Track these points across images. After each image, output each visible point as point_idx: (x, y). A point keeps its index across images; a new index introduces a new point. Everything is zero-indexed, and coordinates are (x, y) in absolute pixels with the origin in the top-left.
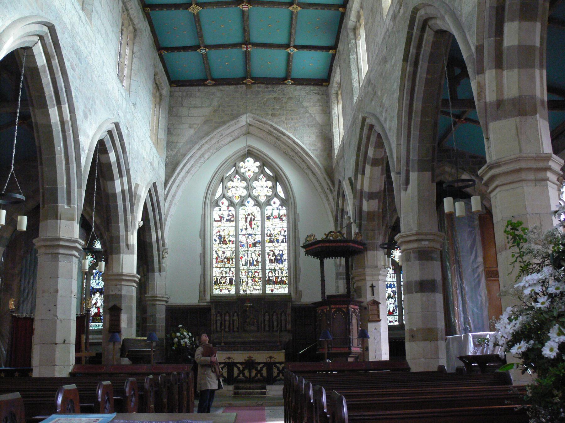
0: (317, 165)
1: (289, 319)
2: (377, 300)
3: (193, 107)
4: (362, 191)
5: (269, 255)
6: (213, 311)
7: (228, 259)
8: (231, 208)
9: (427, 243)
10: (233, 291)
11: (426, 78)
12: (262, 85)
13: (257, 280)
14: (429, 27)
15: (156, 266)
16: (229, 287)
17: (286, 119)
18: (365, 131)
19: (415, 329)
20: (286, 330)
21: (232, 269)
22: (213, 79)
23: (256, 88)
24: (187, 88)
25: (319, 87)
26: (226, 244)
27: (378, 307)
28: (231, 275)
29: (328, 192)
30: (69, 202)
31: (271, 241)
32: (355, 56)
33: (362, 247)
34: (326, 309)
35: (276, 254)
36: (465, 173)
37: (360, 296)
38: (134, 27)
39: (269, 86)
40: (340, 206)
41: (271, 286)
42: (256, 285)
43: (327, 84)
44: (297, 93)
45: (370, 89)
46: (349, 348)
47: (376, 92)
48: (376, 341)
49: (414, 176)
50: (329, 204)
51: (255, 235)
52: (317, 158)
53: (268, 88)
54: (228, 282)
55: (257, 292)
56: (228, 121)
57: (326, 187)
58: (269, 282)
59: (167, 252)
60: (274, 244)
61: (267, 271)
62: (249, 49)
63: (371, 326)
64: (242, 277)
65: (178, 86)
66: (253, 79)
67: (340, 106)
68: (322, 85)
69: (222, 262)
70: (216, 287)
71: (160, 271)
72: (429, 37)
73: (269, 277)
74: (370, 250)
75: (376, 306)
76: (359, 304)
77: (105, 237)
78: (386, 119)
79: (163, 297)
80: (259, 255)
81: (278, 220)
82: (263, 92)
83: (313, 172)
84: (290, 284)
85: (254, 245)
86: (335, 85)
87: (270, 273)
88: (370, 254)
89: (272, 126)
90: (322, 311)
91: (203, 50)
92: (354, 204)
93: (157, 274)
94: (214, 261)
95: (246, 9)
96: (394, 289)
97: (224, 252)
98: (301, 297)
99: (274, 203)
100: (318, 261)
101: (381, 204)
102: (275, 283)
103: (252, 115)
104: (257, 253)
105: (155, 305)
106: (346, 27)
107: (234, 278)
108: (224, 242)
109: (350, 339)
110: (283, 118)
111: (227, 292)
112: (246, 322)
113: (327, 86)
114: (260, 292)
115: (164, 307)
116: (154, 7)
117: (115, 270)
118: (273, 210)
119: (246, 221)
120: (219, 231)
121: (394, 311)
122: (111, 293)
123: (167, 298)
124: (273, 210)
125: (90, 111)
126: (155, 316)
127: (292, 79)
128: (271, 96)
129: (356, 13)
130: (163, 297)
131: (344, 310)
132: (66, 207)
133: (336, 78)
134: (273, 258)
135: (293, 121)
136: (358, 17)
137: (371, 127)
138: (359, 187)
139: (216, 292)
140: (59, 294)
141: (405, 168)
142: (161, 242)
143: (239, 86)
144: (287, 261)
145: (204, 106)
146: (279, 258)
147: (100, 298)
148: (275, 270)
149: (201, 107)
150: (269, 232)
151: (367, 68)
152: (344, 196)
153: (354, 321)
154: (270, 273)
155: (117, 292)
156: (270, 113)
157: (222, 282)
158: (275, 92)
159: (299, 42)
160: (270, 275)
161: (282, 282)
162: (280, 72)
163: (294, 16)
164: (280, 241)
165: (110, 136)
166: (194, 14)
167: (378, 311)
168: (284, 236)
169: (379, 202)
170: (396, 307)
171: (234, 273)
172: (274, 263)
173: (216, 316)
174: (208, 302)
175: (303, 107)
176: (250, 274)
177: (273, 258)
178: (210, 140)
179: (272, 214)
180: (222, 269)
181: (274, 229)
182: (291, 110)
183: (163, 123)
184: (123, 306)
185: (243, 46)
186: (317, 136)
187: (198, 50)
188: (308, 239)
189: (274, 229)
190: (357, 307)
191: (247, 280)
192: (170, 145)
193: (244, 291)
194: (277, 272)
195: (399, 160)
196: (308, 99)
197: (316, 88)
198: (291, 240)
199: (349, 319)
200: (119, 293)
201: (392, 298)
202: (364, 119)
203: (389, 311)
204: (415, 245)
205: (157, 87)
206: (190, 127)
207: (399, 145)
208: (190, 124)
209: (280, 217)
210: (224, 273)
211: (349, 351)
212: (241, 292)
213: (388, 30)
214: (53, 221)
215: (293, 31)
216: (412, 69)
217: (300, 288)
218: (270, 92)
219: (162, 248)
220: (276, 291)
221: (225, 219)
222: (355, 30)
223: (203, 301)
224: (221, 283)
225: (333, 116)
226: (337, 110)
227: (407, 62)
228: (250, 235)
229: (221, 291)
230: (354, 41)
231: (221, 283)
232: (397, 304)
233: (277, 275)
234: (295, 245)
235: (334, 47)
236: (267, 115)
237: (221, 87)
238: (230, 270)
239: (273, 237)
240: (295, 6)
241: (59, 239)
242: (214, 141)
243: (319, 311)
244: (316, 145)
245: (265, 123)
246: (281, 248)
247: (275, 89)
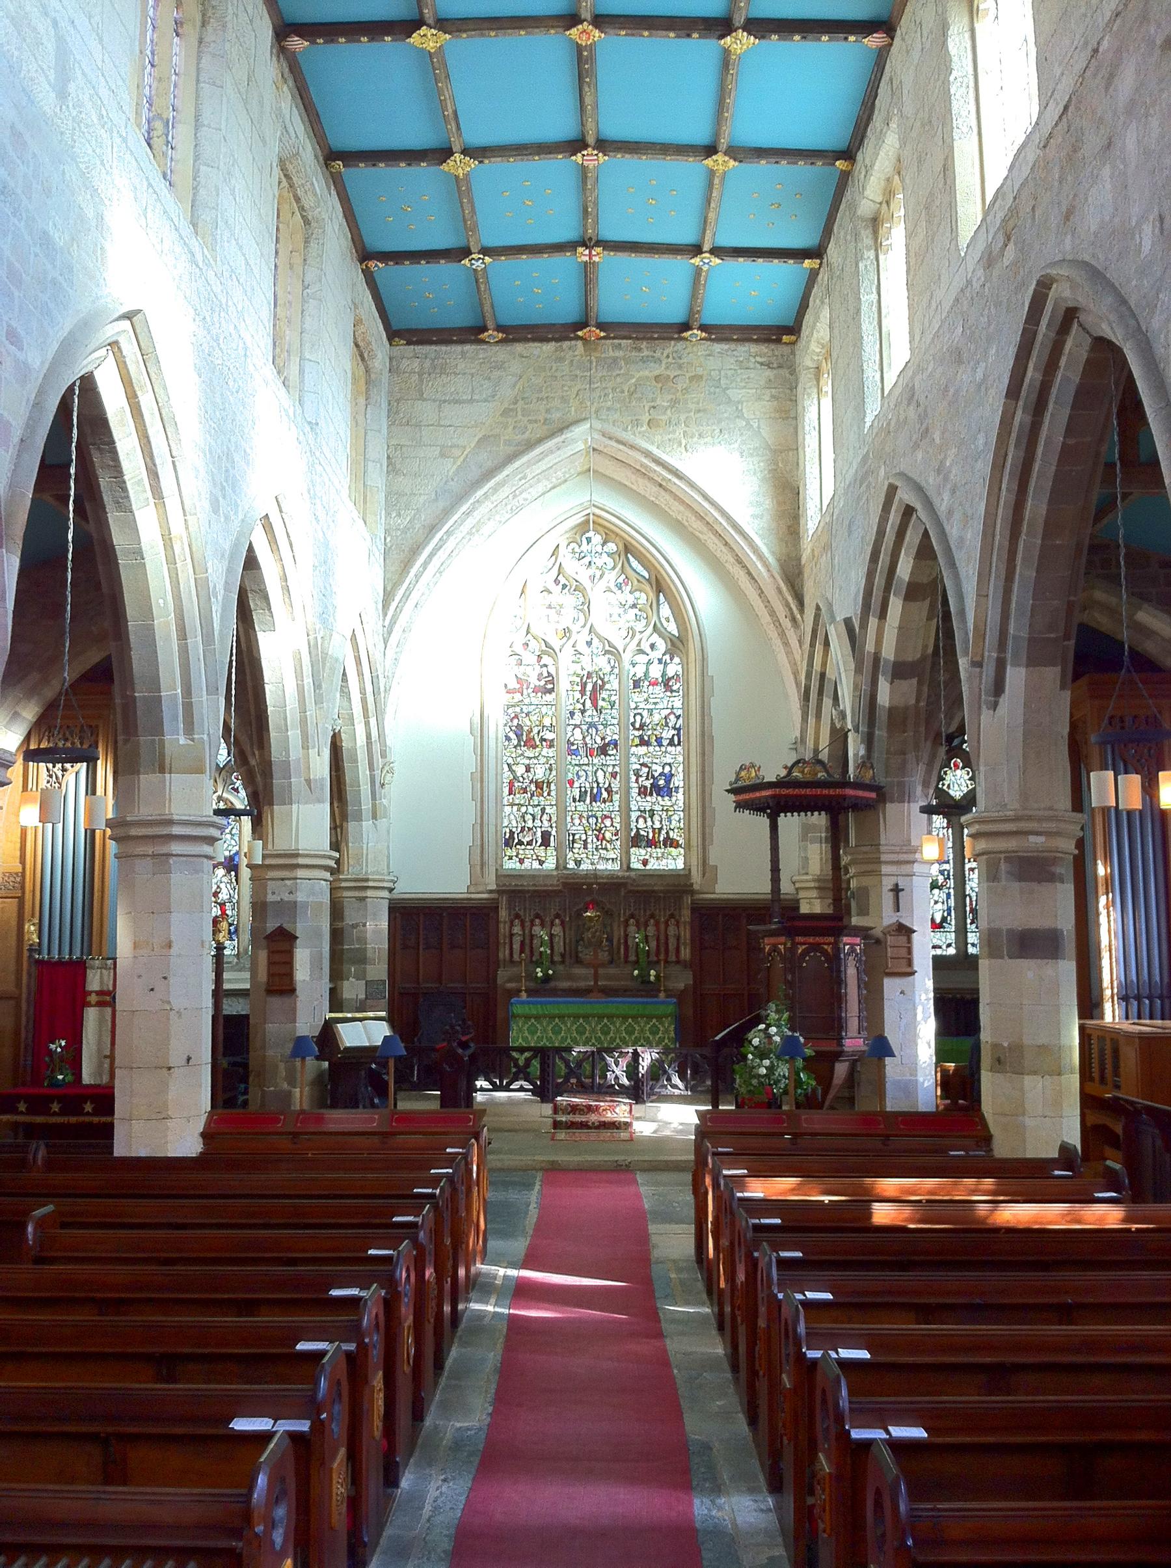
0: (761, 557)
1: (686, 934)
2: (908, 924)
3: (449, 402)
4: (877, 658)
5: (638, 776)
6: (503, 914)
7: (539, 785)
8: (546, 660)
9: (1041, 839)
10: (550, 864)
11: (1064, 444)
13: (608, 835)
14: (1081, 325)
15: (366, 806)
16: (541, 852)
18: (894, 518)
19: (1006, 1044)
20: (678, 962)
21: (548, 810)
22: (500, 328)
23: (609, 350)
24: (434, 347)
25: (773, 346)
26: (535, 747)
27: (909, 941)
28: (546, 824)
29: (787, 623)
30: (189, 729)
31: (644, 742)
32: (874, 296)
33: (873, 795)
34: (785, 944)
35: (656, 774)
36: (1146, 606)
37: (864, 912)
38: (303, 217)
39: (644, 344)
40: (817, 666)
41: (643, 852)
42: (606, 849)
43: (793, 338)
44: (713, 364)
45: (912, 413)
46: (839, 1039)
47: (927, 430)
48: (904, 1021)
49: (1016, 676)
50: (789, 653)
51: (605, 726)
52: (762, 537)
53: (640, 350)
54: (540, 841)
55: (610, 866)
56: (540, 441)
57: (781, 612)
58: (637, 840)
59: (391, 771)
60: (651, 749)
61: (634, 815)
62: (596, 259)
63: (891, 985)
64: (573, 830)
65: (409, 343)
66: (601, 326)
67: (827, 402)
68: (778, 341)
69: (525, 791)
70: (509, 852)
71: (374, 817)
72: (1076, 348)
73: (638, 829)
74: (892, 802)
75: (904, 939)
76: (864, 932)
77: (253, 762)
78: (950, 512)
79: (383, 881)
80: (614, 775)
81: (659, 689)
82: (628, 361)
83: (749, 573)
84: (688, 847)
85: (603, 751)
86: (814, 347)
87: (641, 820)
88: (891, 808)
89: (648, 454)
90: (775, 948)
92: (856, 687)
93: (367, 824)
94: (506, 790)
95: (591, 165)
97: (528, 769)
98: (715, 880)
99: (652, 646)
100: (763, 821)
101: (925, 689)
102: (652, 843)
103: (598, 425)
104: (610, 769)
105: (363, 899)
106: (853, 207)
107: (554, 833)
108: (530, 743)
109: (840, 1018)
110: (679, 432)
111: (536, 865)
112: (582, 939)
113: (794, 343)
114: (617, 866)
115: (386, 903)
117: (281, 843)
118: (649, 663)
119: (583, 692)
120: (516, 717)
121: (944, 919)
122: (270, 898)
123: (392, 881)
124: (649, 663)
125: (223, 488)
126: (364, 925)
127: (703, 328)
128: (647, 373)
130: (383, 881)
131: (829, 948)
132: (182, 741)
133: (818, 330)
134: (648, 784)
135: (702, 441)
136: (889, 195)
137: (909, 511)
138: (870, 647)
139: (511, 865)
140: (174, 950)
141: (995, 655)
142: (376, 748)
143: (566, 344)
144: (681, 790)
145: (475, 397)
146: (662, 782)
147: (225, 879)
148: (652, 813)
149: (471, 401)
150: (638, 718)
151: (905, 355)
152: (827, 644)
153: (851, 972)
154: (641, 820)
155: (287, 897)
156: (646, 418)
157: (525, 841)
159: (727, 240)
160: (641, 824)
161: (670, 842)
162: (674, 312)
163: (716, 181)
164: (665, 743)
166: (457, 177)
167: (909, 951)
168: (674, 728)
169: (920, 683)
170: (949, 909)
171: (554, 819)
172: (651, 794)
173: (512, 925)
174: (491, 892)
175: (729, 401)
176: (592, 821)
177: (648, 784)
178: (495, 489)
179: (646, 674)
180: (523, 809)
181: (650, 711)
182: (699, 411)
183: (378, 449)
184: (300, 929)
185: (580, 250)
186: (764, 479)
187: (466, 262)
188: (743, 774)
189: (650, 711)
190: (858, 940)
191: (584, 837)
192: (394, 501)
193: (578, 863)
194: (656, 818)
195: (980, 634)
196: (739, 371)
197: (763, 348)
198: (693, 740)
199: (839, 971)
200: (291, 898)
201: (940, 888)
202: (892, 490)
203: (933, 920)
204: (1011, 844)
205: (361, 353)
206: (443, 455)
207: (981, 595)
208: (442, 447)
209: (666, 683)
210: (528, 817)
211: (839, 1049)
212: (571, 865)
213: (969, 282)
214: (154, 778)
215: (712, 215)
216: (1028, 419)
217: (712, 862)
218: (643, 360)
219: (379, 762)
220: (653, 865)
221: (532, 686)
222: (875, 222)
223: (481, 889)
224: (520, 843)
226: (818, 413)
227: (1017, 399)
228: (591, 725)
229: (521, 861)
231: (520, 843)
232: (952, 902)
233: (657, 825)
234: (703, 754)
235: (816, 253)
236: (637, 423)
237: (519, 348)
238: (543, 810)
239: (650, 733)
240: (720, 157)
241: (171, 822)
242: (506, 491)
243: (767, 948)
244: (759, 504)
245: (632, 447)
246: (668, 760)
247: (658, 354)
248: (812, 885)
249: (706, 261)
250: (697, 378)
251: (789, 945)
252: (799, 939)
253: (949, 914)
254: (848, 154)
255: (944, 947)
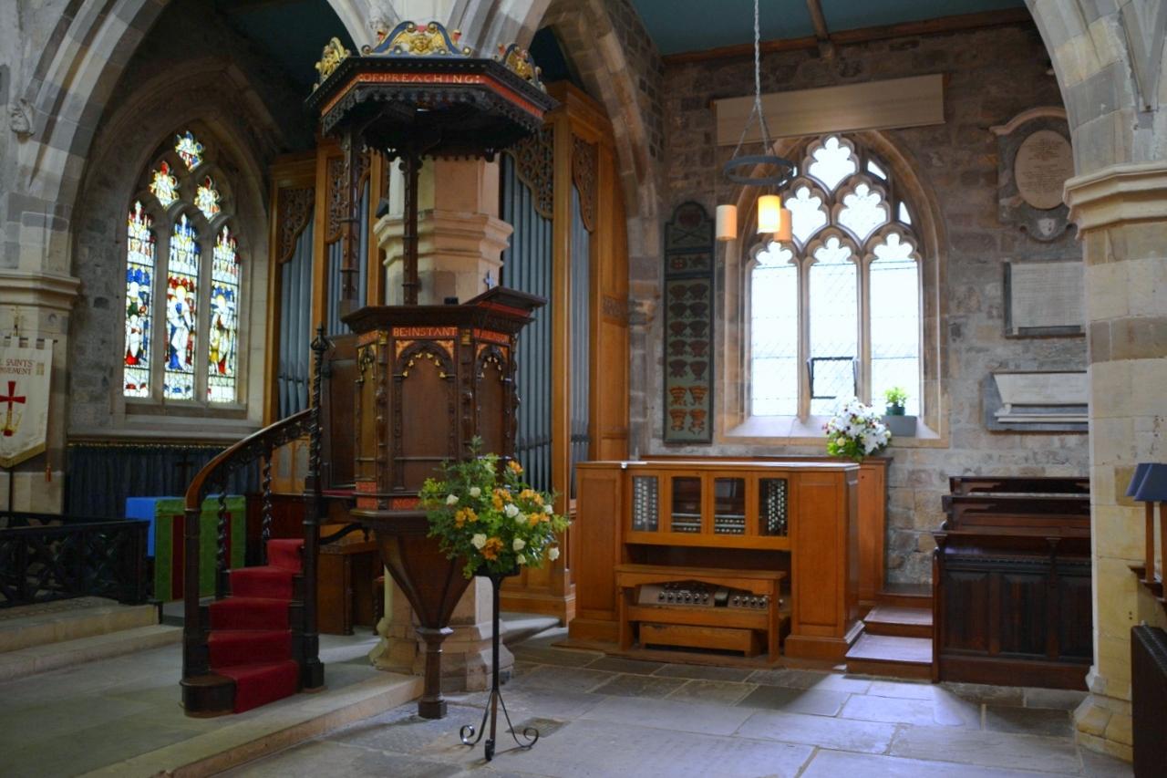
96: (146, 289)
121: (140, 353)
170: (145, 342)
201: (138, 314)
232: (148, 334)
248: (30, 285)
251: (466, 340)
252: (397, 332)
253: (145, 348)
255: (138, 387)
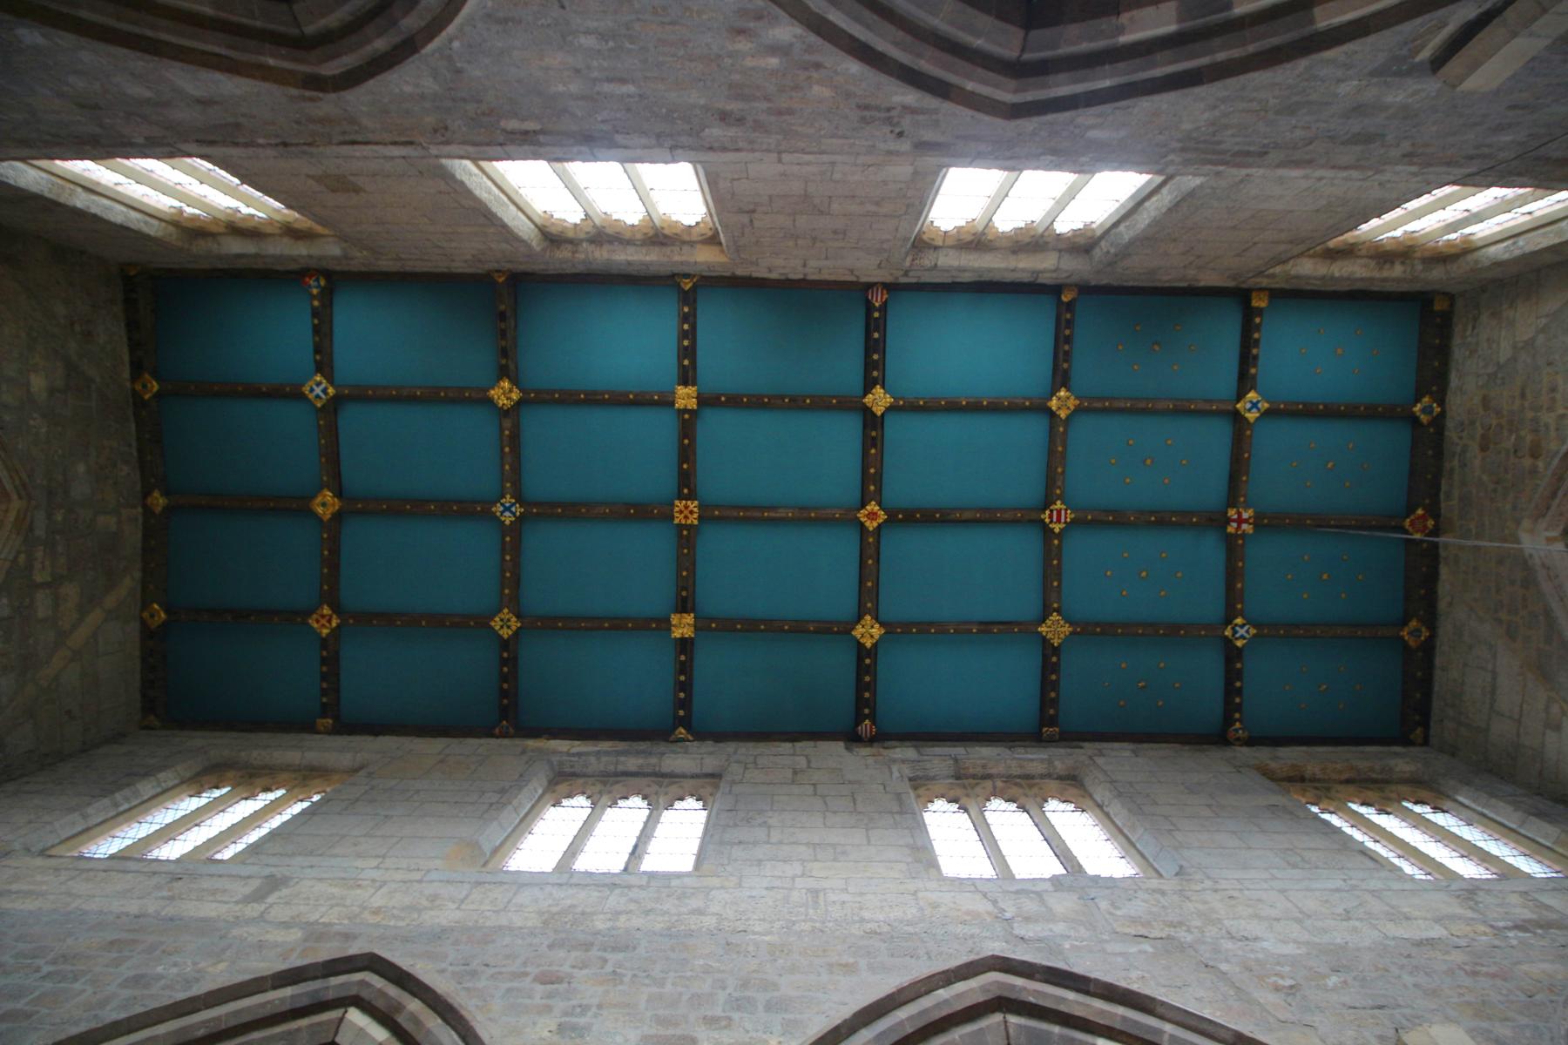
12: (1444, 487)
17: (1551, 409)
32: (1122, 228)
39: (1447, 465)
53: (1452, 471)
91: (1235, 632)
103: (1526, 523)
116: (1046, 720)
128: (1477, 462)
129: (1022, 256)
156: (1527, 462)
158: (1465, 449)
163: (1098, 405)
165: (1018, 1013)
175: (1514, 359)
182: (1523, 396)
197: (1458, 329)
218: (1463, 465)
225: (1517, 252)
230: (1103, 243)
235: (1240, 296)
236: (1533, 471)
237: (1442, 605)
249: (1248, 406)
250: (1485, 401)
254: (1055, 290)
